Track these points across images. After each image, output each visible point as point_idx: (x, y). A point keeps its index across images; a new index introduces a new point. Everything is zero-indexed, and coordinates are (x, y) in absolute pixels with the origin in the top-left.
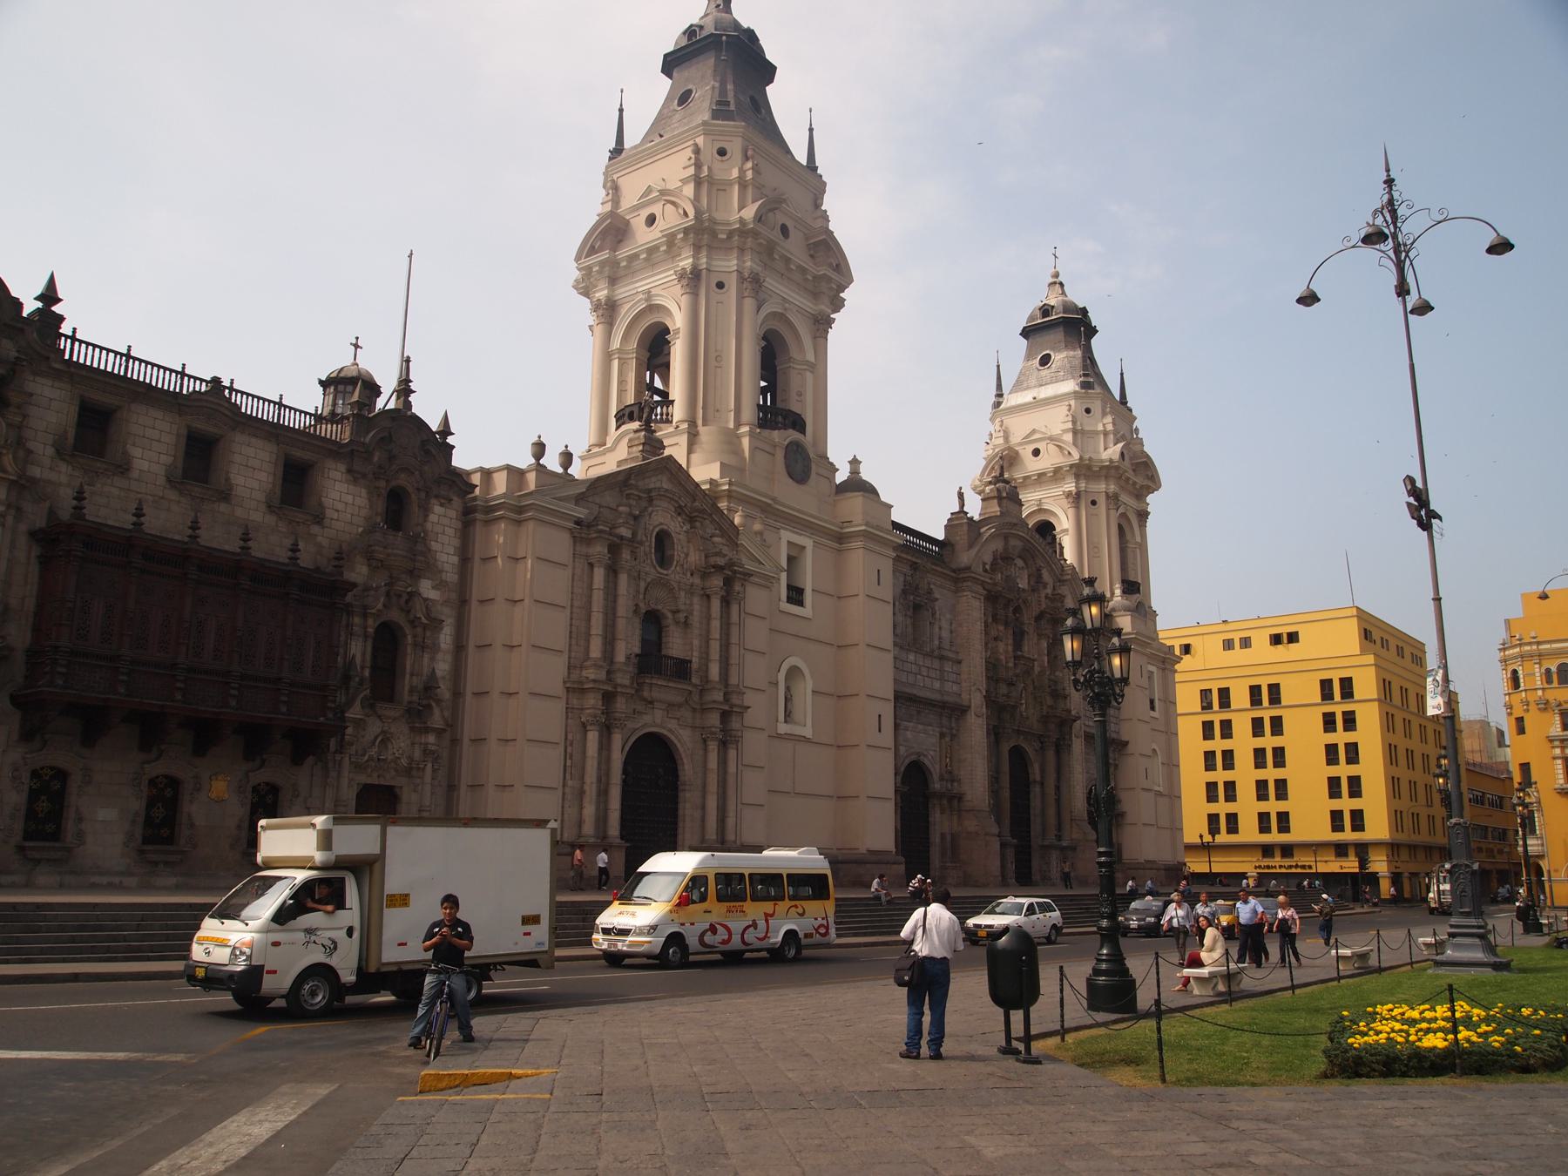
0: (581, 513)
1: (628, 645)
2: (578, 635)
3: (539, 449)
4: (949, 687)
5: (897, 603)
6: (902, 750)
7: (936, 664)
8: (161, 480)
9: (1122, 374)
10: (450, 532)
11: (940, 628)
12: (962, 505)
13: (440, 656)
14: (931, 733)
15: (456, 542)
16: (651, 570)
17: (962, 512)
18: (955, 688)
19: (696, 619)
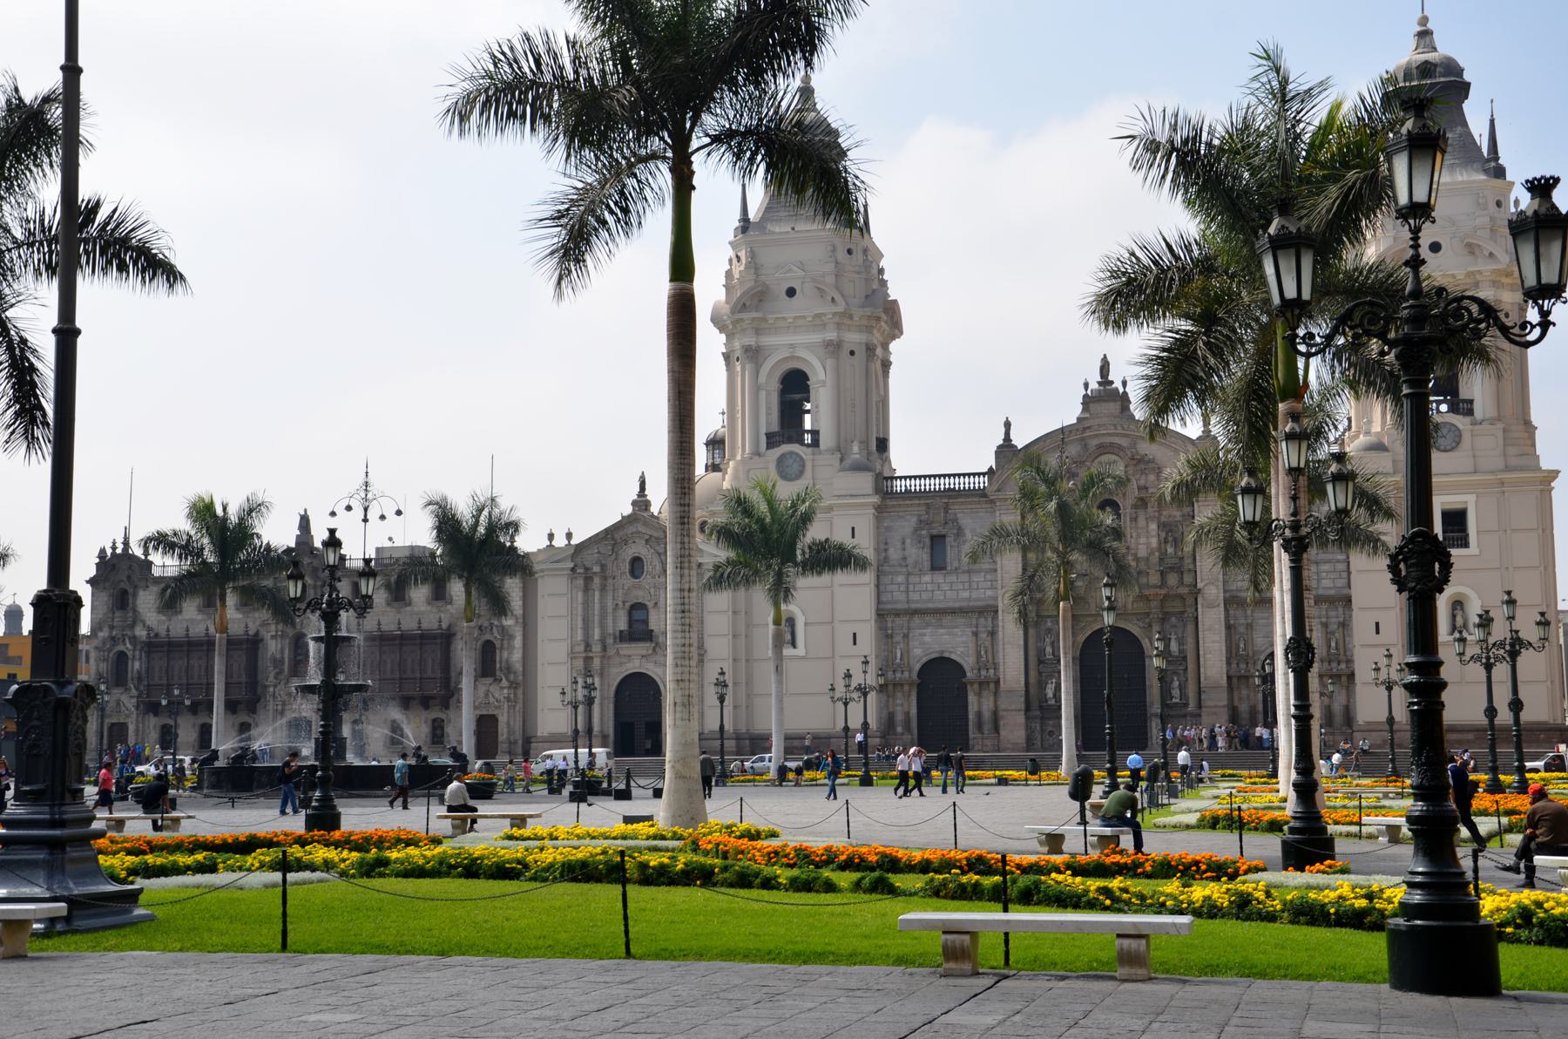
0: (571, 565)
1: (623, 625)
2: (572, 629)
3: (551, 536)
4: (974, 595)
5: (908, 541)
6: (917, 652)
7: (964, 577)
8: (384, 604)
9: (1492, 122)
10: (517, 590)
12: (1007, 433)
13: (515, 651)
15: (521, 594)
16: (629, 581)
17: (1007, 438)
18: (989, 593)
19: (661, 603)
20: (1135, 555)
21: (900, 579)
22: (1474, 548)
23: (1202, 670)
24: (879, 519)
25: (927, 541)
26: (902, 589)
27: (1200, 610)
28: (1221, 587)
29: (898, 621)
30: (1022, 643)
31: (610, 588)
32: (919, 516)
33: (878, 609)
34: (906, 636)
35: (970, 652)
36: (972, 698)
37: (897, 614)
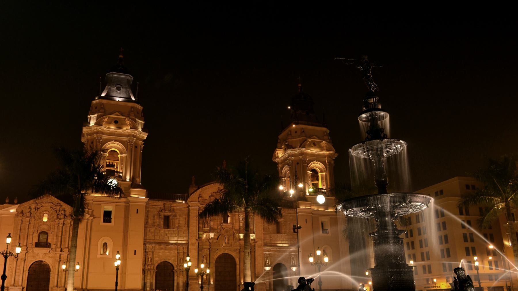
5: (156, 217)
11: (179, 221)
14: (173, 253)
20: (235, 228)
21: (153, 230)
22: (330, 234)
23: (256, 269)
24: (146, 208)
25: (163, 217)
26: (153, 234)
27: (256, 249)
28: (263, 241)
29: (150, 246)
30: (197, 257)
31: (32, 224)
32: (160, 207)
33: (144, 242)
34: (153, 252)
35: (177, 260)
36: (176, 277)
37: (151, 243)
